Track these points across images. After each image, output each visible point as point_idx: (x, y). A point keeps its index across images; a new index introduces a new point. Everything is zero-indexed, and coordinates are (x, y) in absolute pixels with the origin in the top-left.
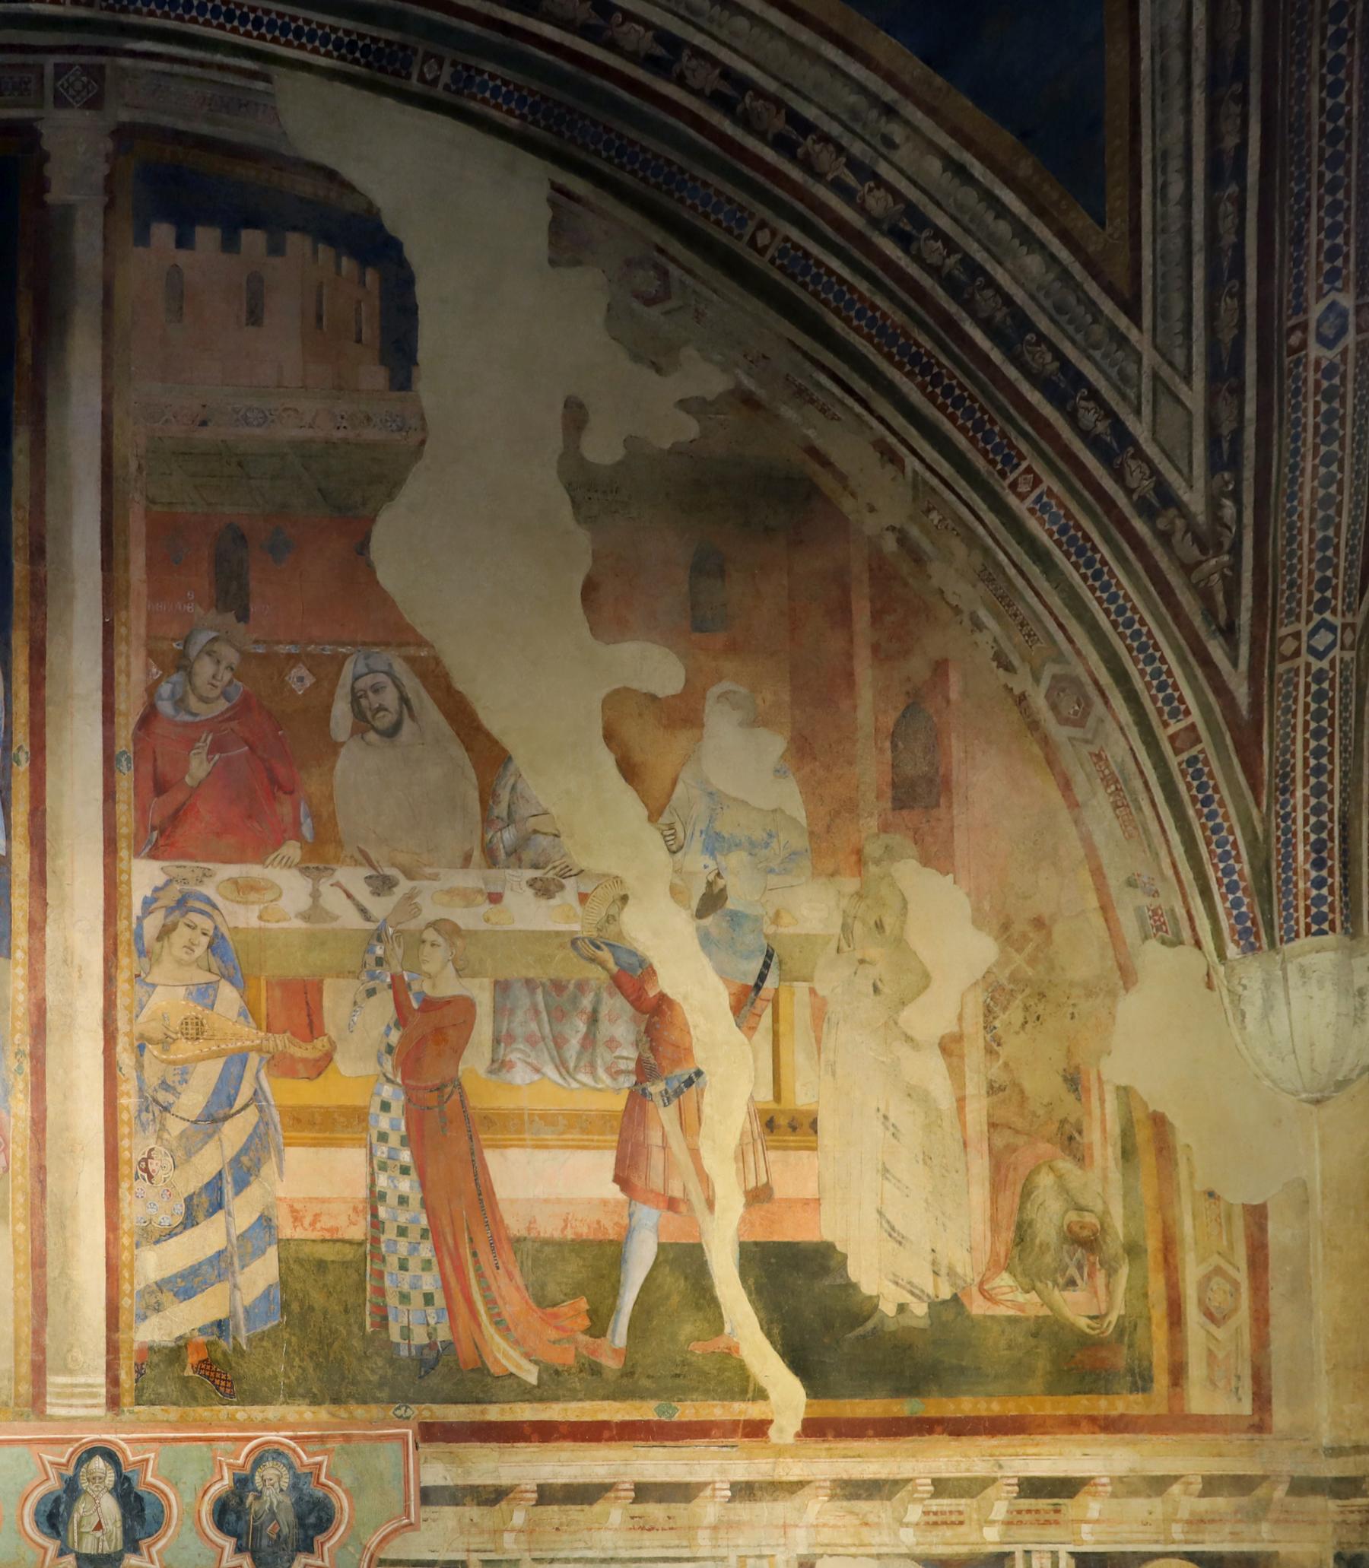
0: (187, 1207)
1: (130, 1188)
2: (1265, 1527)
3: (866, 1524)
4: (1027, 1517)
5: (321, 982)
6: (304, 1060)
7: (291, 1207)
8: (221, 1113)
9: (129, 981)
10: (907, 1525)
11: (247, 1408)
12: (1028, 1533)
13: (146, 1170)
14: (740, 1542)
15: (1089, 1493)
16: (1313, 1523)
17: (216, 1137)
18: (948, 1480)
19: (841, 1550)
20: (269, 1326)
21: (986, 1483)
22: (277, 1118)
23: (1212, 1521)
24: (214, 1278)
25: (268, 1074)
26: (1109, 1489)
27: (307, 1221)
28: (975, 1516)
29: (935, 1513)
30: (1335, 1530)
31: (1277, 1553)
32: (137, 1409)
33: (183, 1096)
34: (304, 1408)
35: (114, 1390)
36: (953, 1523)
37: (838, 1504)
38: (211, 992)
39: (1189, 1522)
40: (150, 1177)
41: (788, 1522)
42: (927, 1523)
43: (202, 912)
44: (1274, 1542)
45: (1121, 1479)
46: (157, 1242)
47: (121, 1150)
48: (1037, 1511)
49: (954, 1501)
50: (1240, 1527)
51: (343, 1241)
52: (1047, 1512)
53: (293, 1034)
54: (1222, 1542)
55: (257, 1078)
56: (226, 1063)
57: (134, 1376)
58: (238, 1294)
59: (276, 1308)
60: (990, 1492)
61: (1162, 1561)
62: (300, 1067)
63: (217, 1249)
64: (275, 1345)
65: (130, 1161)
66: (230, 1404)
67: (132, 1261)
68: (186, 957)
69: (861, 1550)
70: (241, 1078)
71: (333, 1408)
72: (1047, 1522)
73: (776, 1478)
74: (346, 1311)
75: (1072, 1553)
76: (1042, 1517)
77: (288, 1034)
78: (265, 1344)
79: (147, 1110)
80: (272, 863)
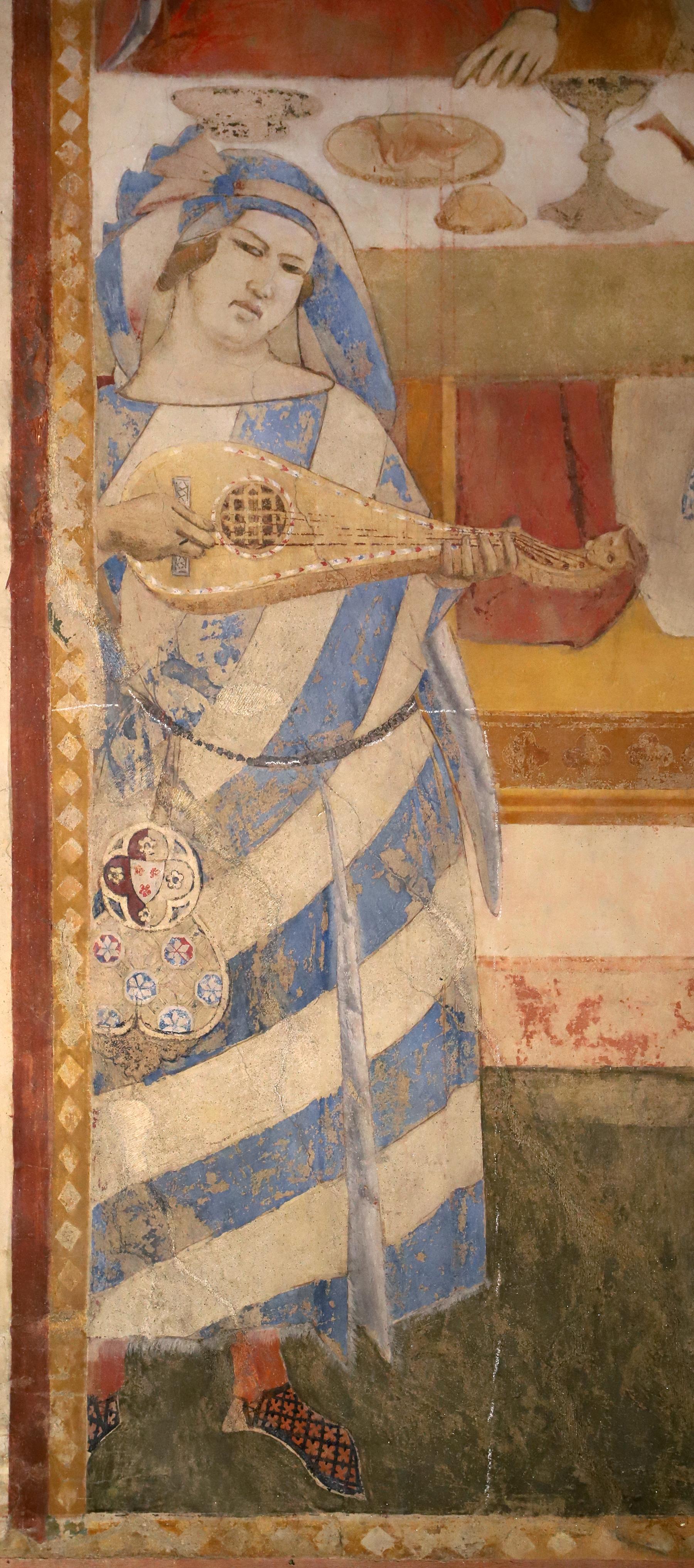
0: (234, 985)
1: (82, 936)
5: (609, 388)
6: (558, 596)
7: (519, 982)
8: (330, 737)
9: (84, 395)
11: (393, 1520)
13: (125, 888)
17: (316, 801)
20: (454, 1299)
22: (482, 749)
24: (306, 1170)
25: (460, 633)
27: (560, 1023)
32: (93, 1520)
33: (225, 694)
34: (548, 1522)
35: (30, 1471)
38: (304, 418)
40: (136, 906)
43: (283, 211)
46: (152, 1076)
47: (55, 836)
51: (660, 1073)
53: (529, 527)
55: (429, 644)
56: (345, 604)
57: (88, 1431)
58: (371, 1212)
59: (477, 1250)
62: (547, 613)
63: (315, 1094)
64: (471, 1349)
65: (80, 867)
66: (349, 1507)
67: (84, 1127)
68: (236, 329)
70: (384, 644)
71: (631, 1523)
74: (668, 1260)
77: (516, 528)
78: (442, 1346)
79: (129, 732)
80: (476, 75)
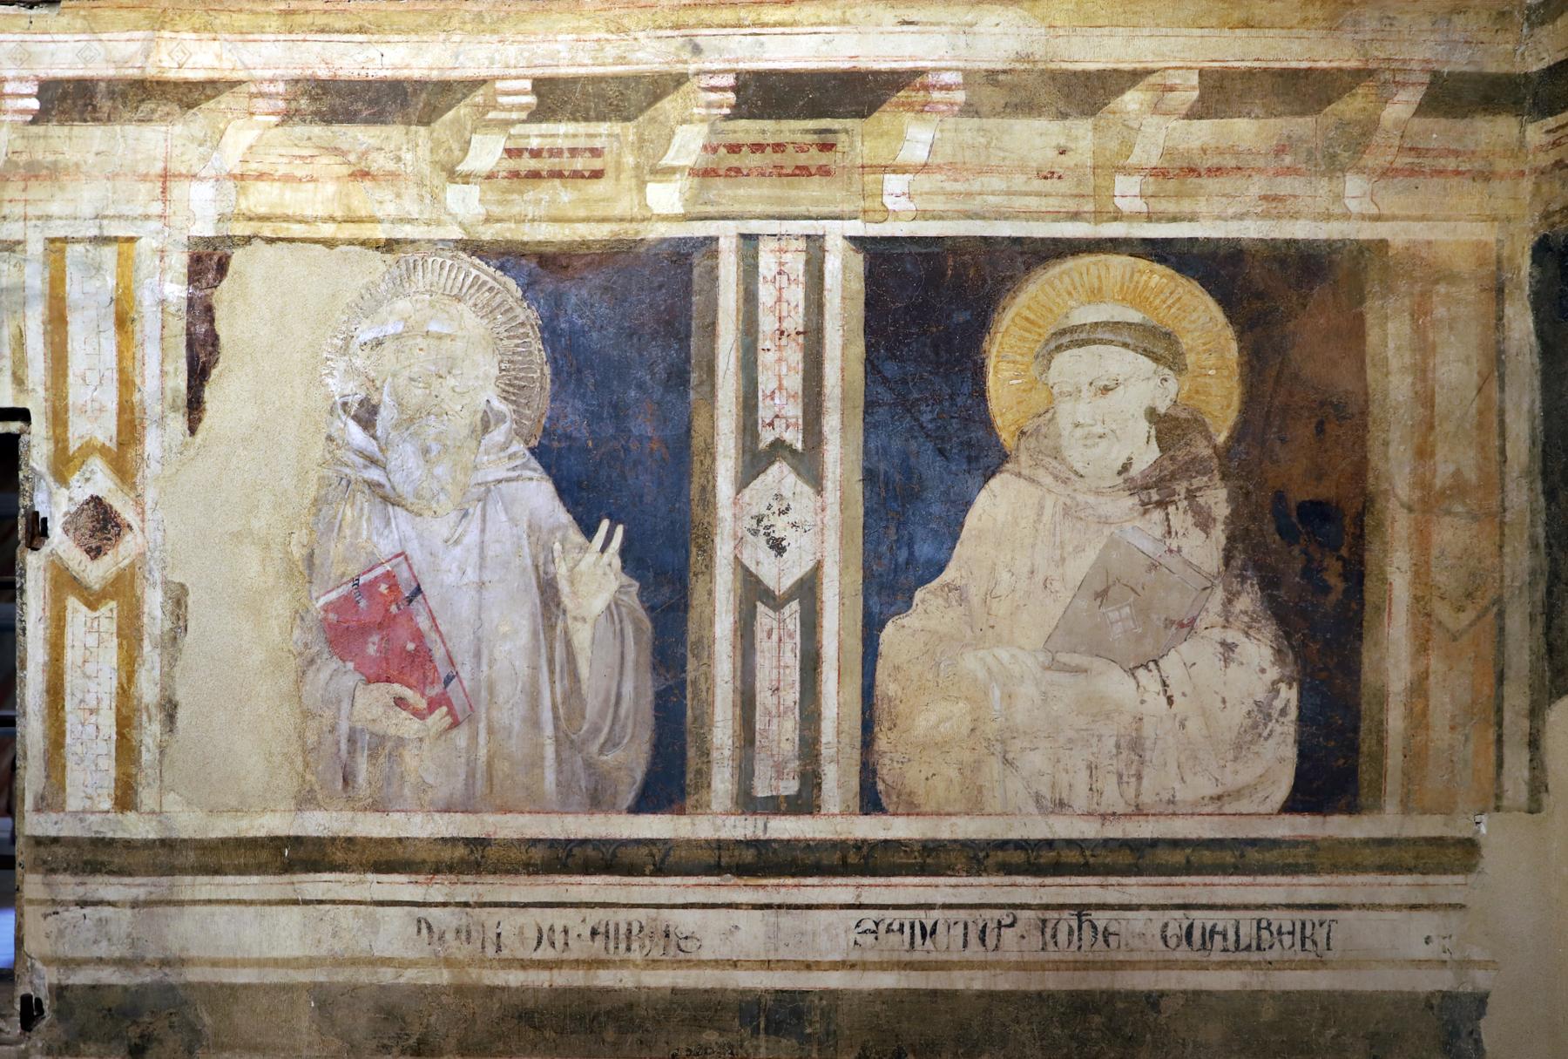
2: (1354, 185)
3: (365, 174)
4: (755, 160)
10: (466, 178)
12: (752, 194)
14: (54, 208)
15: (909, 106)
16: (1486, 176)
18: (575, 80)
19: (297, 230)
21: (660, 86)
23: (1217, 171)
26: (960, 96)
28: (629, 160)
29: (536, 154)
30: (1537, 186)
31: (1383, 244)
36: (577, 175)
37: (300, 130)
39: (1160, 173)
41: (177, 167)
42: (515, 175)
44: (1378, 218)
45: (991, 76)
48: (779, 147)
49: (581, 128)
50: (1286, 186)
52: (801, 149)
54: (1241, 217)
60: (669, 105)
61: (1086, 260)
69: (348, 231)
72: (803, 171)
73: (151, 72)
75: (852, 239)
76: (790, 159)
